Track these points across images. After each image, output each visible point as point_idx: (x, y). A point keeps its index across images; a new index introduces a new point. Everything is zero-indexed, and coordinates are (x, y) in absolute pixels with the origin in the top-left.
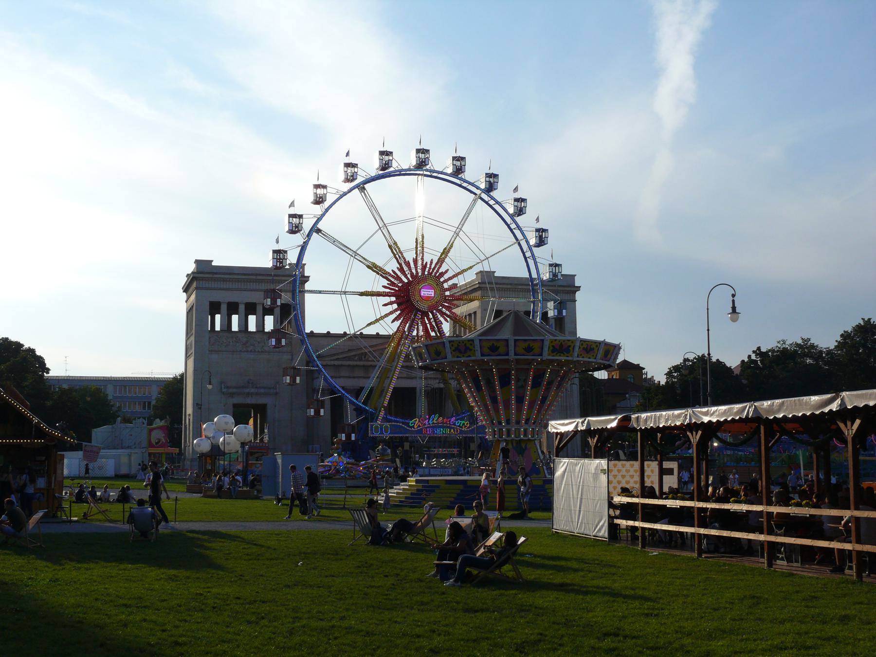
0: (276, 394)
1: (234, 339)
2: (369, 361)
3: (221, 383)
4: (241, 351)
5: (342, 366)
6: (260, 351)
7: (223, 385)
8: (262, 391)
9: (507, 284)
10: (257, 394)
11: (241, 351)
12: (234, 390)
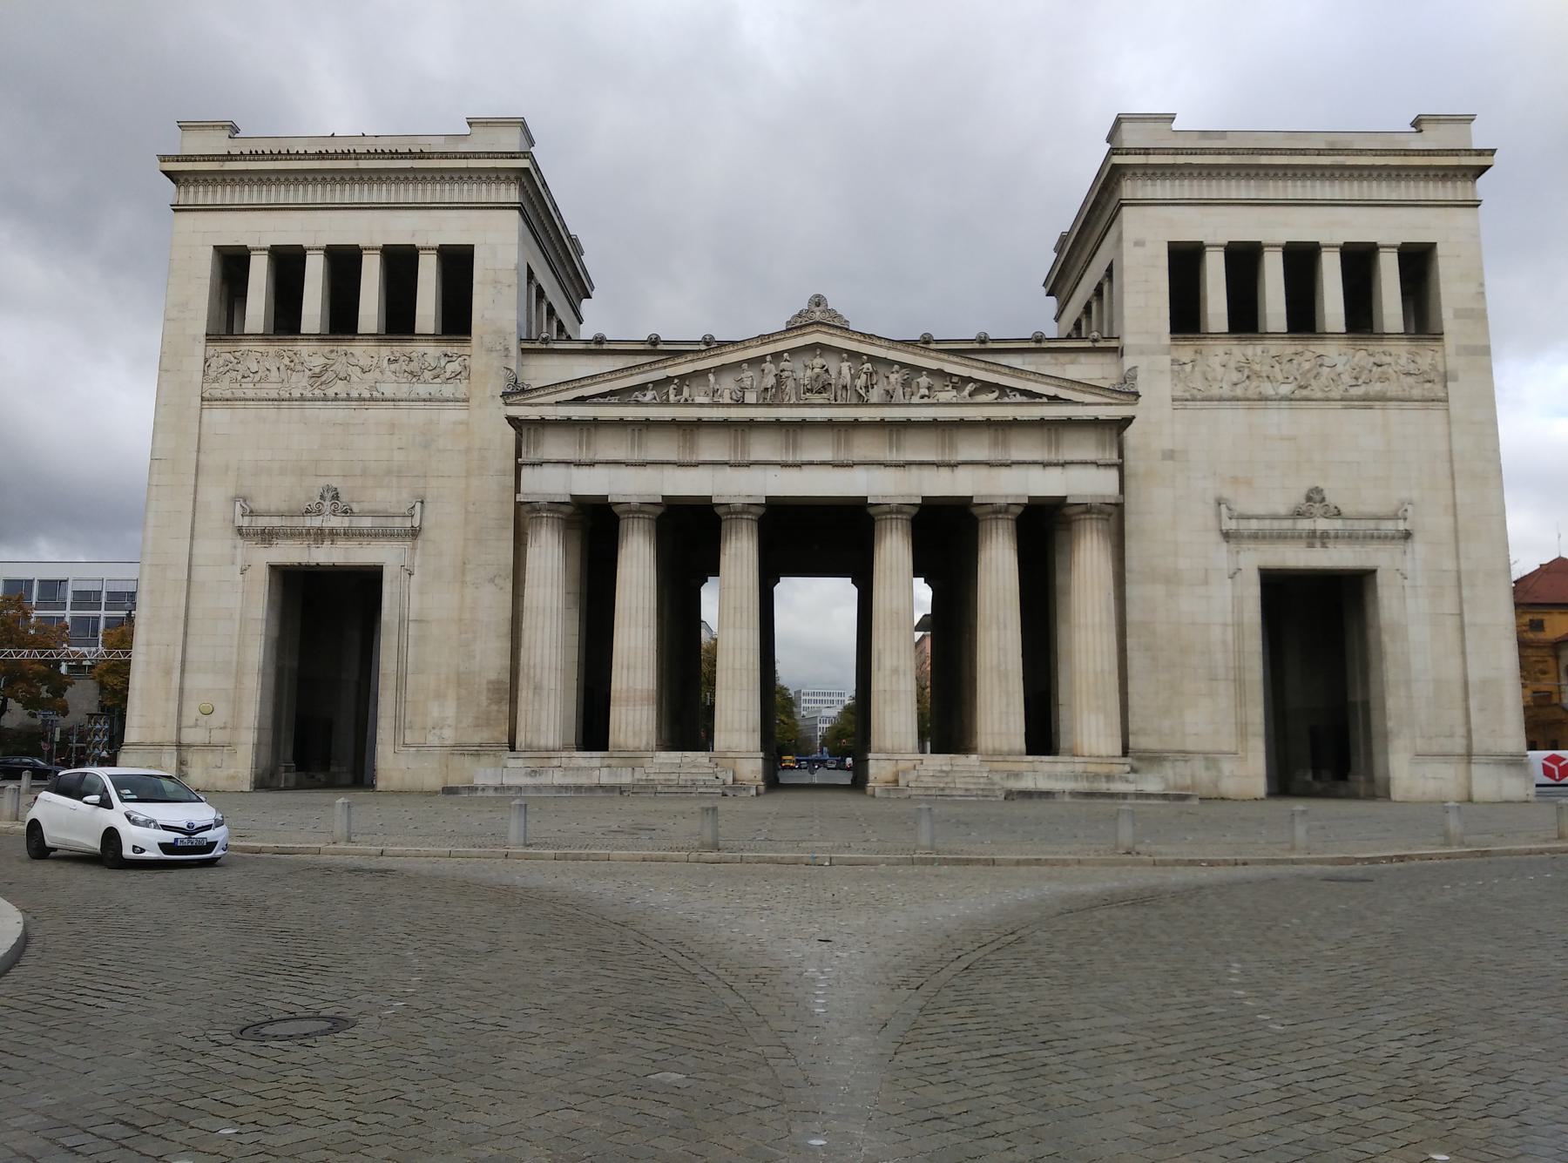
0: (415, 533)
1: (287, 361)
2: (693, 405)
3: (235, 499)
4: (302, 398)
5: (596, 424)
6: (366, 394)
7: (238, 504)
8: (366, 523)
9: (1219, 152)
10: (349, 534)
11: (302, 398)
12: (276, 522)
